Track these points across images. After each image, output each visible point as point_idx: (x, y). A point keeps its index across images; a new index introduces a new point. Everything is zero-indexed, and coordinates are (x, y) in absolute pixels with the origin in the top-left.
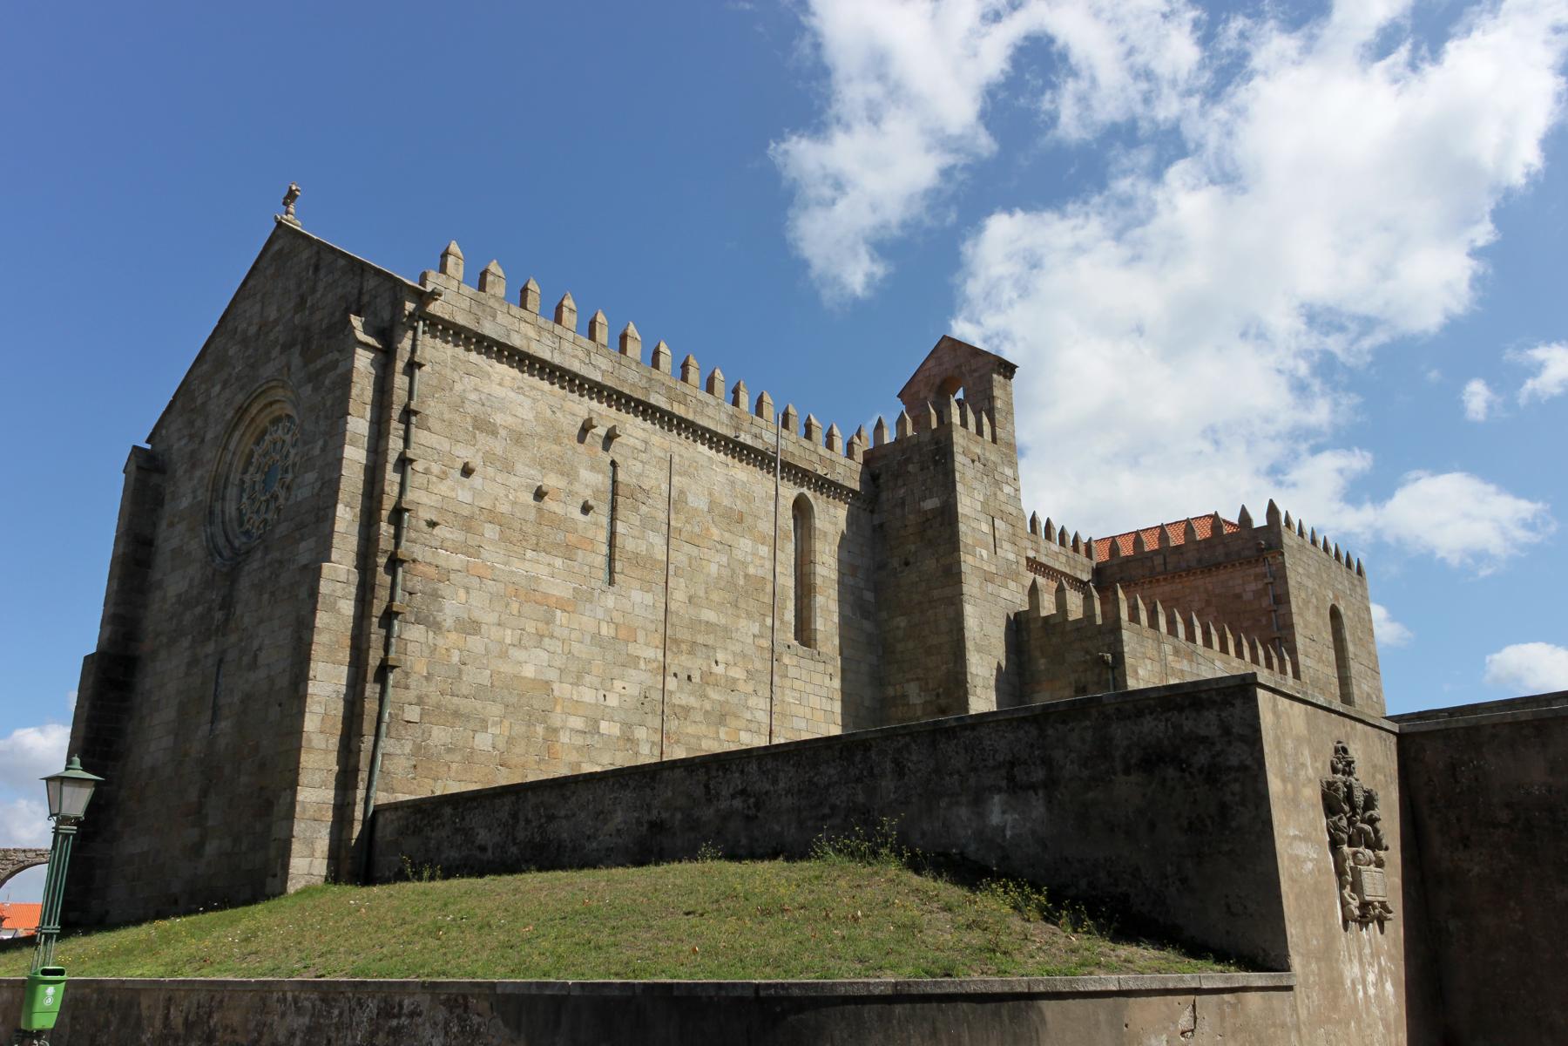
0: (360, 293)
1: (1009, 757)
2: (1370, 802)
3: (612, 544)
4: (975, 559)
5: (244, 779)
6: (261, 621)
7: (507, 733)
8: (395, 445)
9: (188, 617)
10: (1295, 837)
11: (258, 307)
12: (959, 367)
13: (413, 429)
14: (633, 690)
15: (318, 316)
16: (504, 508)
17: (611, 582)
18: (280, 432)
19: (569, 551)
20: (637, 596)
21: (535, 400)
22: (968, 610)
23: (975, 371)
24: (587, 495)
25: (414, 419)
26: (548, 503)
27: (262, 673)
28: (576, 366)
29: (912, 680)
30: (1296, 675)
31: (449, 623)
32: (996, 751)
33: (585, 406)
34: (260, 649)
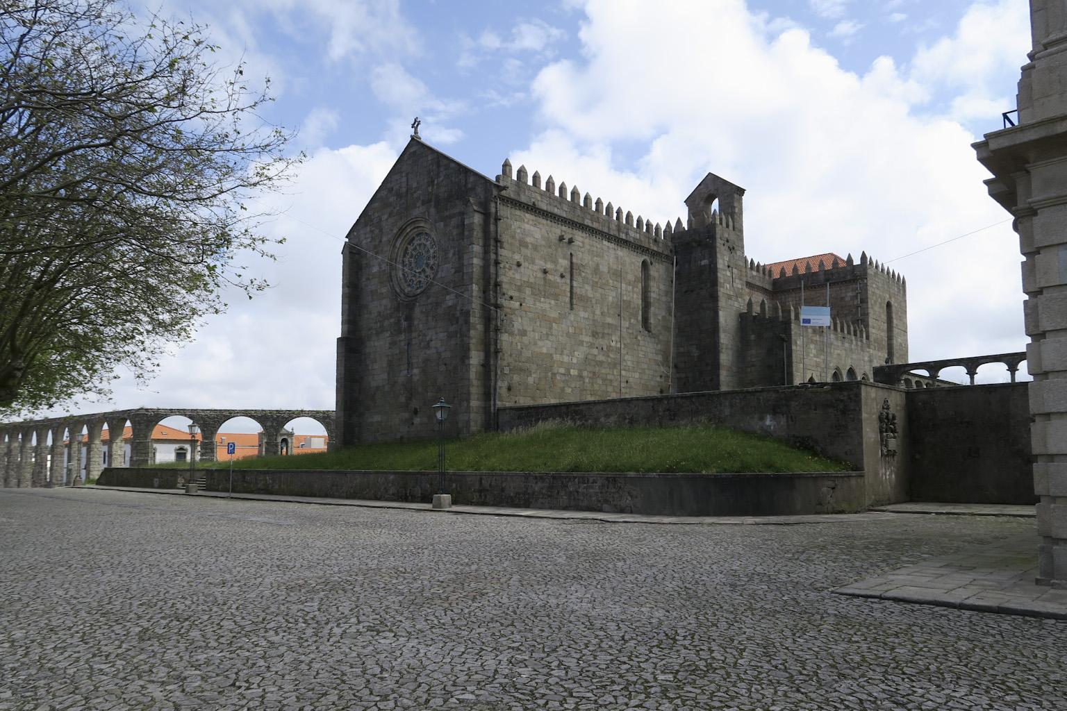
2: (894, 417)
3: (571, 292)
4: (724, 289)
8: (493, 256)
12: (717, 190)
13: (499, 249)
14: (582, 356)
16: (532, 280)
17: (572, 309)
19: (556, 297)
20: (582, 314)
22: (721, 313)
24: (562, 270)
25: (499, 244)
26: (550, 277)
27: (433, 351)
28: (556, 211)
30: (868, 338)
31: (516, 332)
33: (558, 230)
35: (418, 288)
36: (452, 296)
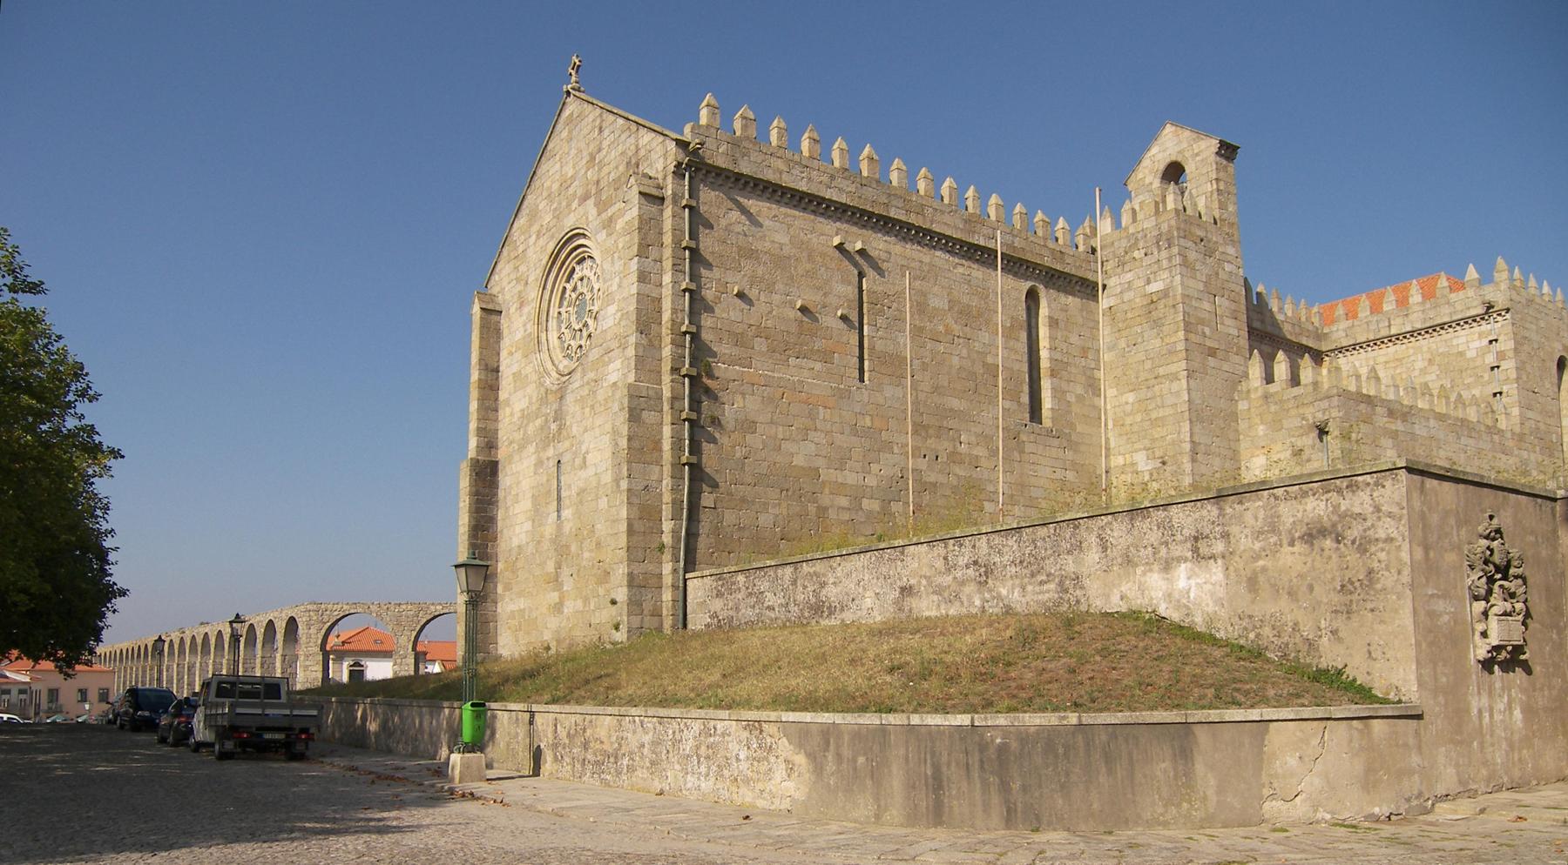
1: (1193, 533)
5: (586, 555)
6: (586, 430)
7: (785, 513)
9: (531, 429)
10: (1432, 596)
11: (558, 165)
15: (606, 170)
19: (826, 356)
21: (789, 226)
23: (1197, 155)
27: (590, 471)
29: (1140, 450)
34: (587, 452)
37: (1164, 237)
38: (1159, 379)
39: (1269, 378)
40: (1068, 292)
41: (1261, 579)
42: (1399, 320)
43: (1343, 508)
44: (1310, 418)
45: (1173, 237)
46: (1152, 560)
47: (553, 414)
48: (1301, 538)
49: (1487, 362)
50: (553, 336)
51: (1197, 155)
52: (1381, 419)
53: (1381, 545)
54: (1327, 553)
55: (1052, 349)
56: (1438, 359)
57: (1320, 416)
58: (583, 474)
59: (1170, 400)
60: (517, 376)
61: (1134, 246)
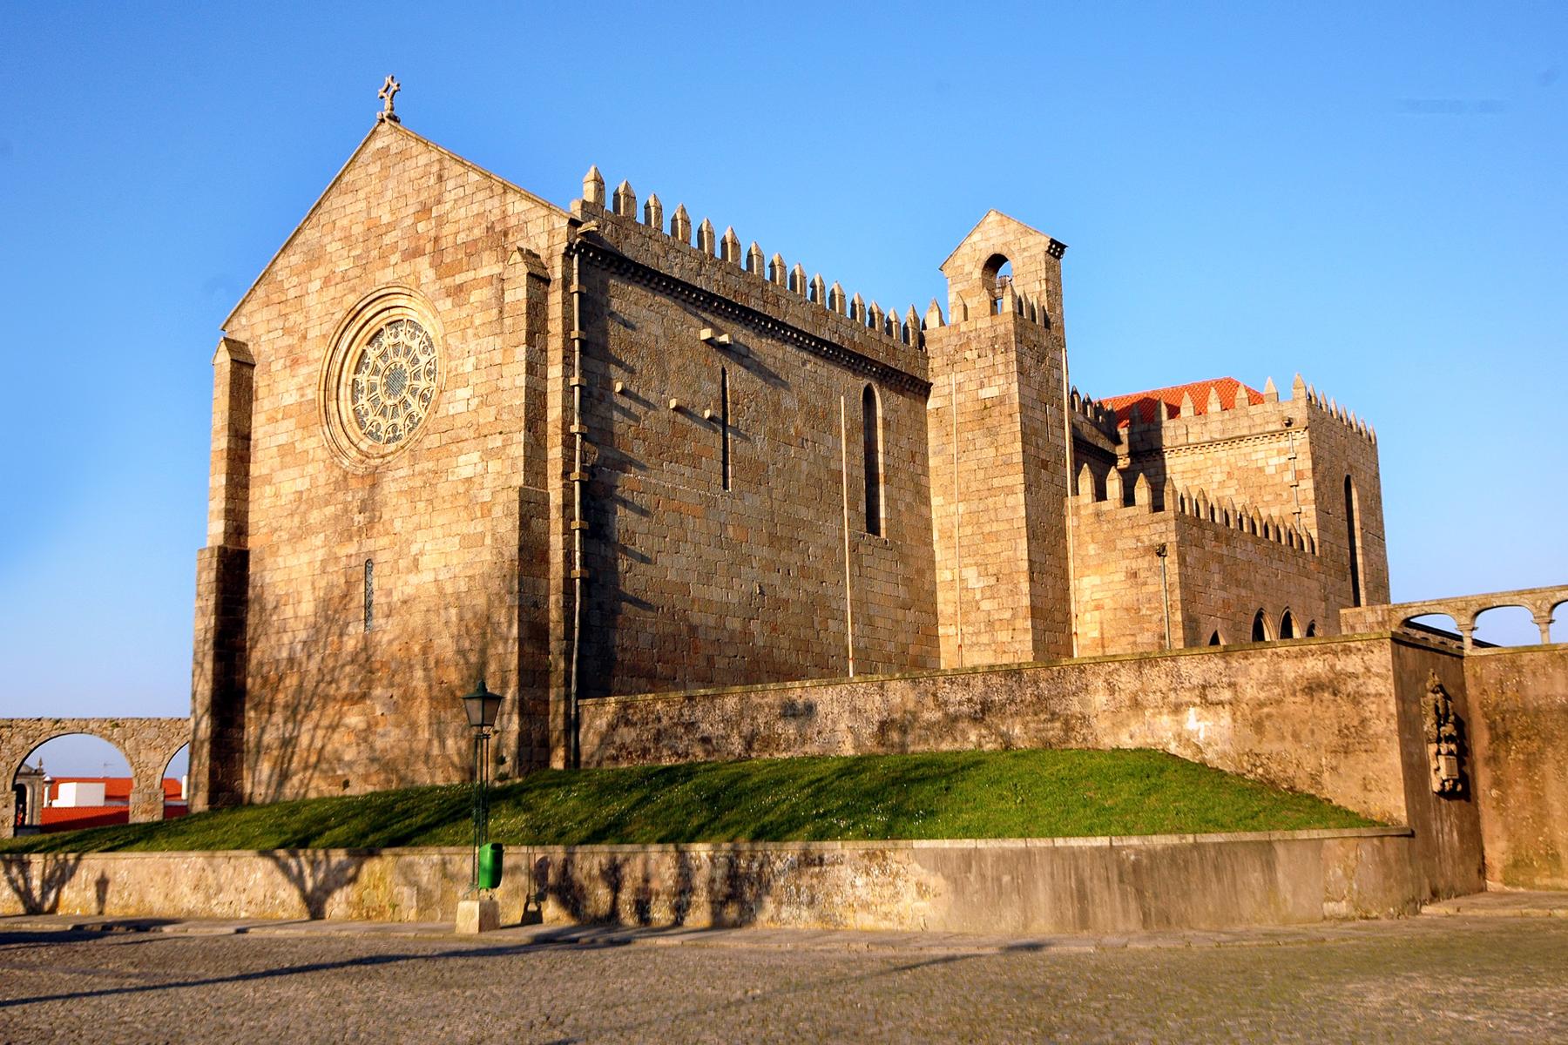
0: (504, 217)
6: (419, 528)
11: (362, 205)
15: (448, 229)
18: (401, 335)
19: (694, 460)
23: (1024, 250)
32: (1191, 677)
34: (422, 553)
35: (389, 441)
36: (475, 457)
37: (1000, 341)
38: (992, 492)
39: (1100, 494)
40: (901, 392)
41: (1267, 723)
42: (1197, 429)
43: (1338, 668)
44: (1146, 539)
45: (1010, 342)
46: (1161, 704)
47: (357, 503)
48: (1303, 690)
49: (1286, 480)
50: (347, 409)
51: (1024, 250)
52: (1210, 545)
53: (1372, 699)
54: (1326, 703)
55: (887, 453)
56: (1236, 472)
57: (1156, 538)
58: (414, 579)
59: (1007, 514)
60: (285, 451)
61: (966, 345)
